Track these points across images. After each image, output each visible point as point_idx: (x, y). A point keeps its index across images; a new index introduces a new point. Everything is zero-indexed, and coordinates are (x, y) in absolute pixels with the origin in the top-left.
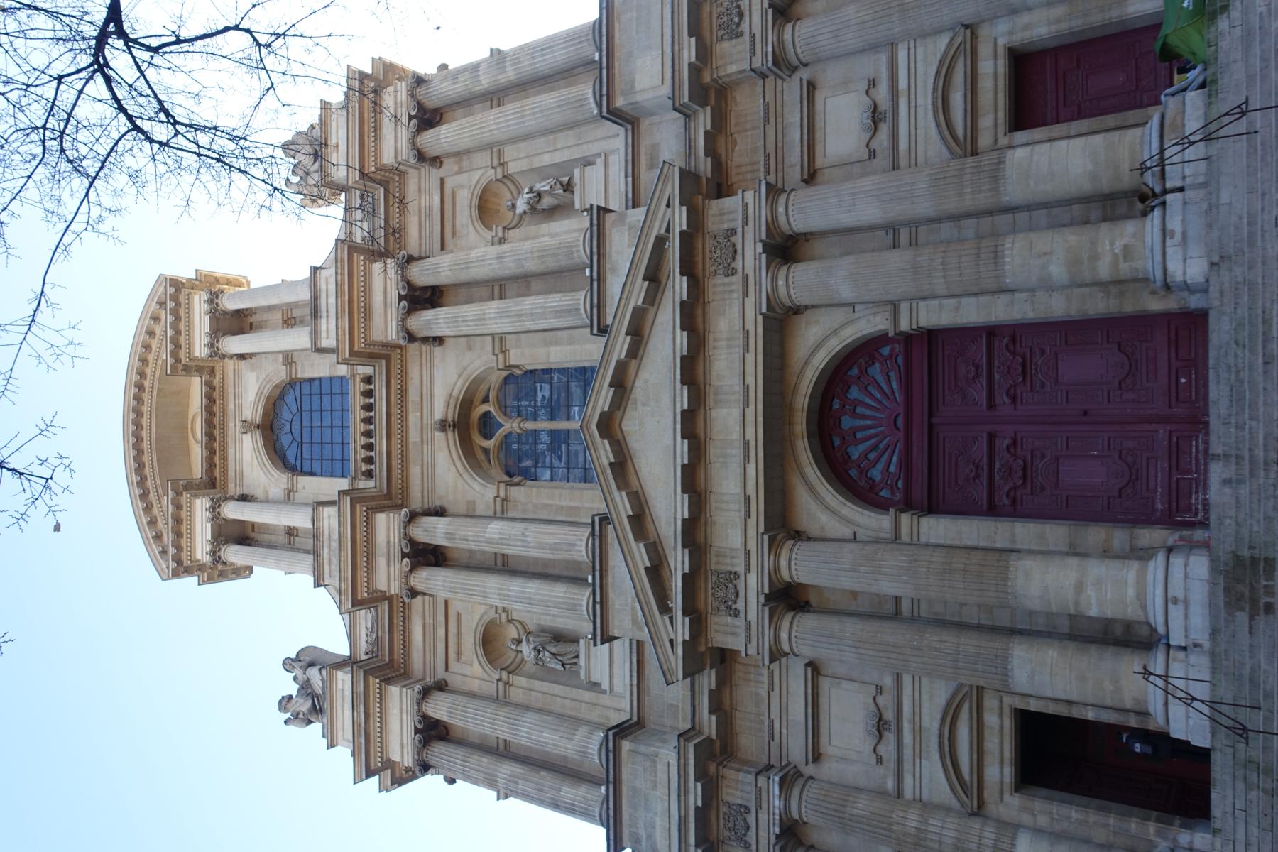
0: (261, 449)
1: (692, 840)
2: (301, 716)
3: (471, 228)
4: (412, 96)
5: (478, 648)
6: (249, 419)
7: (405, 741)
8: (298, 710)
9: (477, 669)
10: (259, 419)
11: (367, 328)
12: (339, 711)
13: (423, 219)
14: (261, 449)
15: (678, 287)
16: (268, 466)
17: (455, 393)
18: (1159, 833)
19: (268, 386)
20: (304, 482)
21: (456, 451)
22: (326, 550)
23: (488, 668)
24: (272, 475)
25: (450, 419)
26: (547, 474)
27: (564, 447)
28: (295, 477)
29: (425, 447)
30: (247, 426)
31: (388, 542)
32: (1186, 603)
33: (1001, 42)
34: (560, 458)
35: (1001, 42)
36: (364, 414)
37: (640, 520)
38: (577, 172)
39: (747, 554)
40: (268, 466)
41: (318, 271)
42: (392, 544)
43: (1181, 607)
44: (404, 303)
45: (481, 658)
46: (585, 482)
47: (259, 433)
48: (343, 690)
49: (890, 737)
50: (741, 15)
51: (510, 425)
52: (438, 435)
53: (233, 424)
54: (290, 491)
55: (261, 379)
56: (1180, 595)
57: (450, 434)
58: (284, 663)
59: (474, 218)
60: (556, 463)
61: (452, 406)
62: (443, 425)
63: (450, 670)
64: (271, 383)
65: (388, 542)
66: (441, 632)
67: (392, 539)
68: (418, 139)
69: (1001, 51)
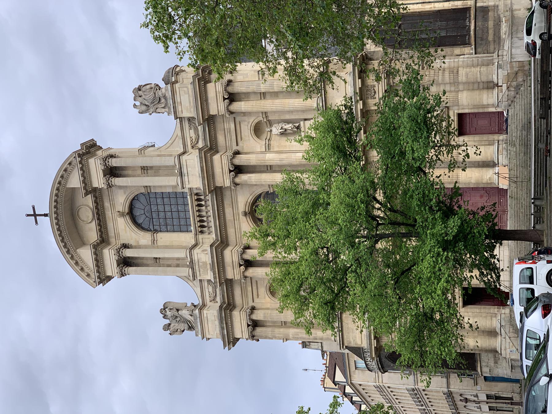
0: (130, 223)
1: (373, 338)
2: (179, 330)
3: (251, 138)
4: (225, 90)
5: (268, 292)
6: (121, 210)
7: (243, 330)
8: (177, 328)
9: (268, 299)
10: (127, 210)
11: (214, 182)
12: (206, 325)
14: (130, 223)
16: (136, 230)
17: (249, 201)
18: (498, 311)
19: (132, 196)
20: (160, 235)
22: (197, 266)
23: (273, 298)
24: (140, 234)
25: (247, 211)
28: (155, 234)
29: (236, 222)
30: (122, 214)
31: (233, 261)
32: (504, 260)
33: (456, 112)
35: (456, 112)
36: (197, 208)
38: (302, 123)
40: (136, 230)
41: (181, 157)
42: (234, 262)
43: (503, 261)
44: (232, 173)
45: (269, 296)
47: (128, 217)
50: (375, 92)
52: (243, 218)
53: (111, 212)
54: (154, 241)
55: (127, 195)
56: (502, 259)
57: (248, 217)
58: (163, 311)
59: (253, 135)
61: (247, 206)
62: (245, 214)
63: (254, 302)
64: (133, 194)
65: (233, 261)
67: (234, 260)
69: (455, 114)
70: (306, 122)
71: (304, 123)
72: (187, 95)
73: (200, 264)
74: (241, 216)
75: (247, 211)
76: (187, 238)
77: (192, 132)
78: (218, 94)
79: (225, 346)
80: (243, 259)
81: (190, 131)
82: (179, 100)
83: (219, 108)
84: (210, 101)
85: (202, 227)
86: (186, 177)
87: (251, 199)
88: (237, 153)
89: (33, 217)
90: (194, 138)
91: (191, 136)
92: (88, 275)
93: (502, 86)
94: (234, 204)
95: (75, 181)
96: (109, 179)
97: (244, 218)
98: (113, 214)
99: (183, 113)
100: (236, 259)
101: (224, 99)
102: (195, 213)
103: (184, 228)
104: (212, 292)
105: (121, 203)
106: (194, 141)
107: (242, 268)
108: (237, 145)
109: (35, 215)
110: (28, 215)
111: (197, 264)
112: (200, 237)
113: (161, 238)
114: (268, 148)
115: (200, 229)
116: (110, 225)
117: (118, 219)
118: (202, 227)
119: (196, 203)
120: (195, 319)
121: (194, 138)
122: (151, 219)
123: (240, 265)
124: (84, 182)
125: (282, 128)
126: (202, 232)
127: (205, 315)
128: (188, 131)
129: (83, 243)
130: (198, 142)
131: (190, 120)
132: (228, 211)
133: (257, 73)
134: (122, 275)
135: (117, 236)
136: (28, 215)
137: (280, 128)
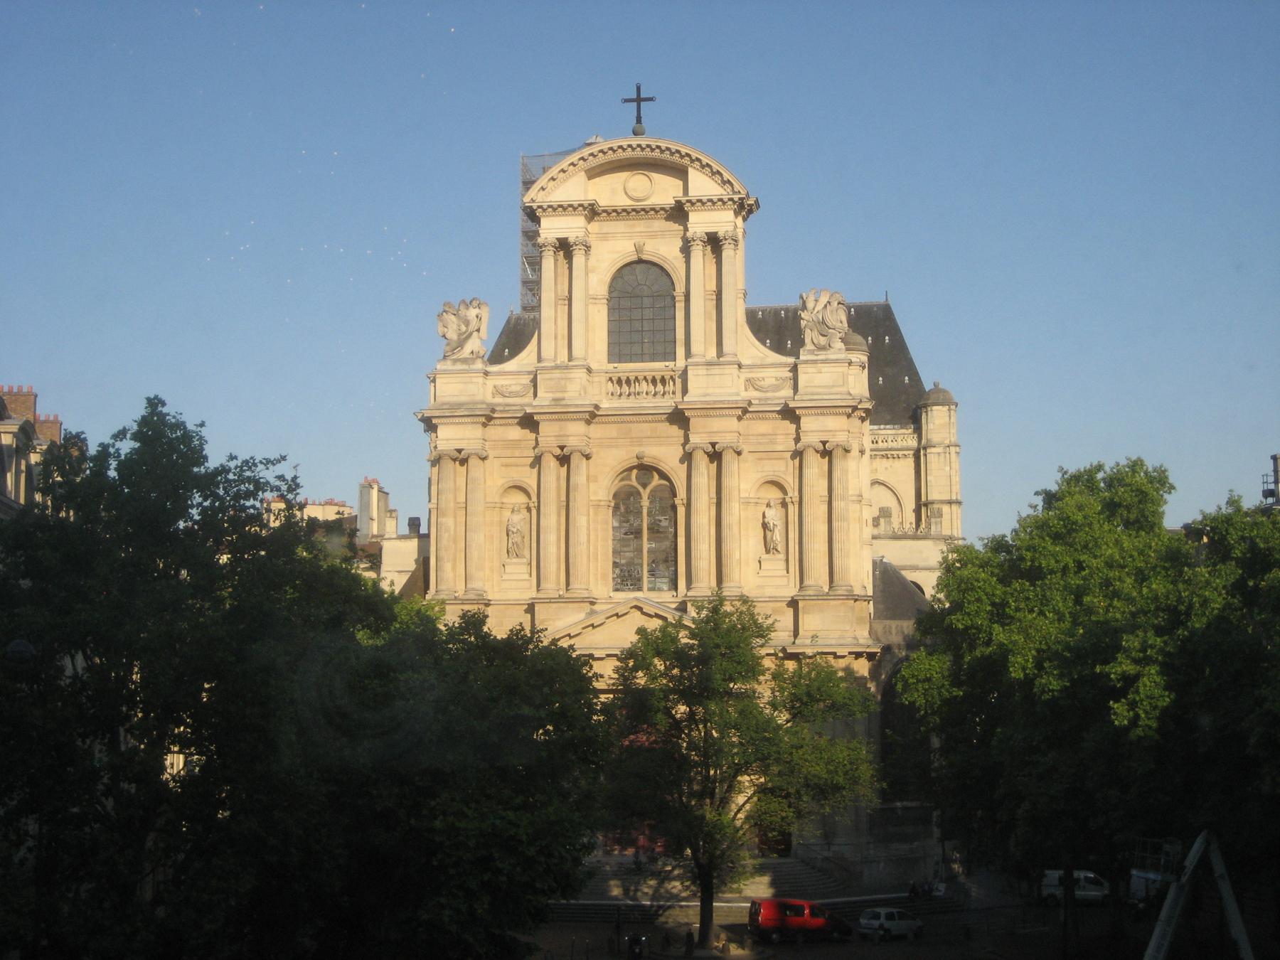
8: (449, 327)
9: (500, 482)
10: (645, 257)
13: (769, 437)
17: (662, 464)
21: (627, 465)
26: (616, 524)
27: (632, 536)
30: (638, 249)
34: (626, 534)
46: (613, 552)
47: (634, 258)
48: (472, 382)
51: (645, 494)
55: (673, 261)
60: (623, 531)
66: (517, 453)
68: (811, 449)
71: (781, 560)
72: (831, 384)
73: (563, 382)
74: (637, 450)
77: (773, 381)
78: (831, 433)
81: (774, 379)
82: (823, 370)
83: (811, 434)
84: (821, 418)
86: (705, 372)
87: (664, 467)
89: (635, 96)
90: (762, 383)
91: (766, 379)
93: (829, 850)
98: (639, 234)
99: (804, 375)
101: (824, 443)
102: (641, 374)
103: (618, 352)
104: (510, 390)
105: (658, 250)
106: (758, 383)
109: (639, 100)
110: (638, 89)
111: (563, 375)
112: (604, 378)
113: (599, 311)
114: (747, 502)
116: (619, 226)
117: (633, 242)
119: (658, 378)
120: (465, 361)
121: (762, 383)
122: (629, 295)
123: (562, 448)
127: (475, 380)
128: (774, 374)
130: (756, 390)
132: (645, 428)
133: (857, 493)
135: (604, 237)
136: (638, 89)
137: (775, 523)
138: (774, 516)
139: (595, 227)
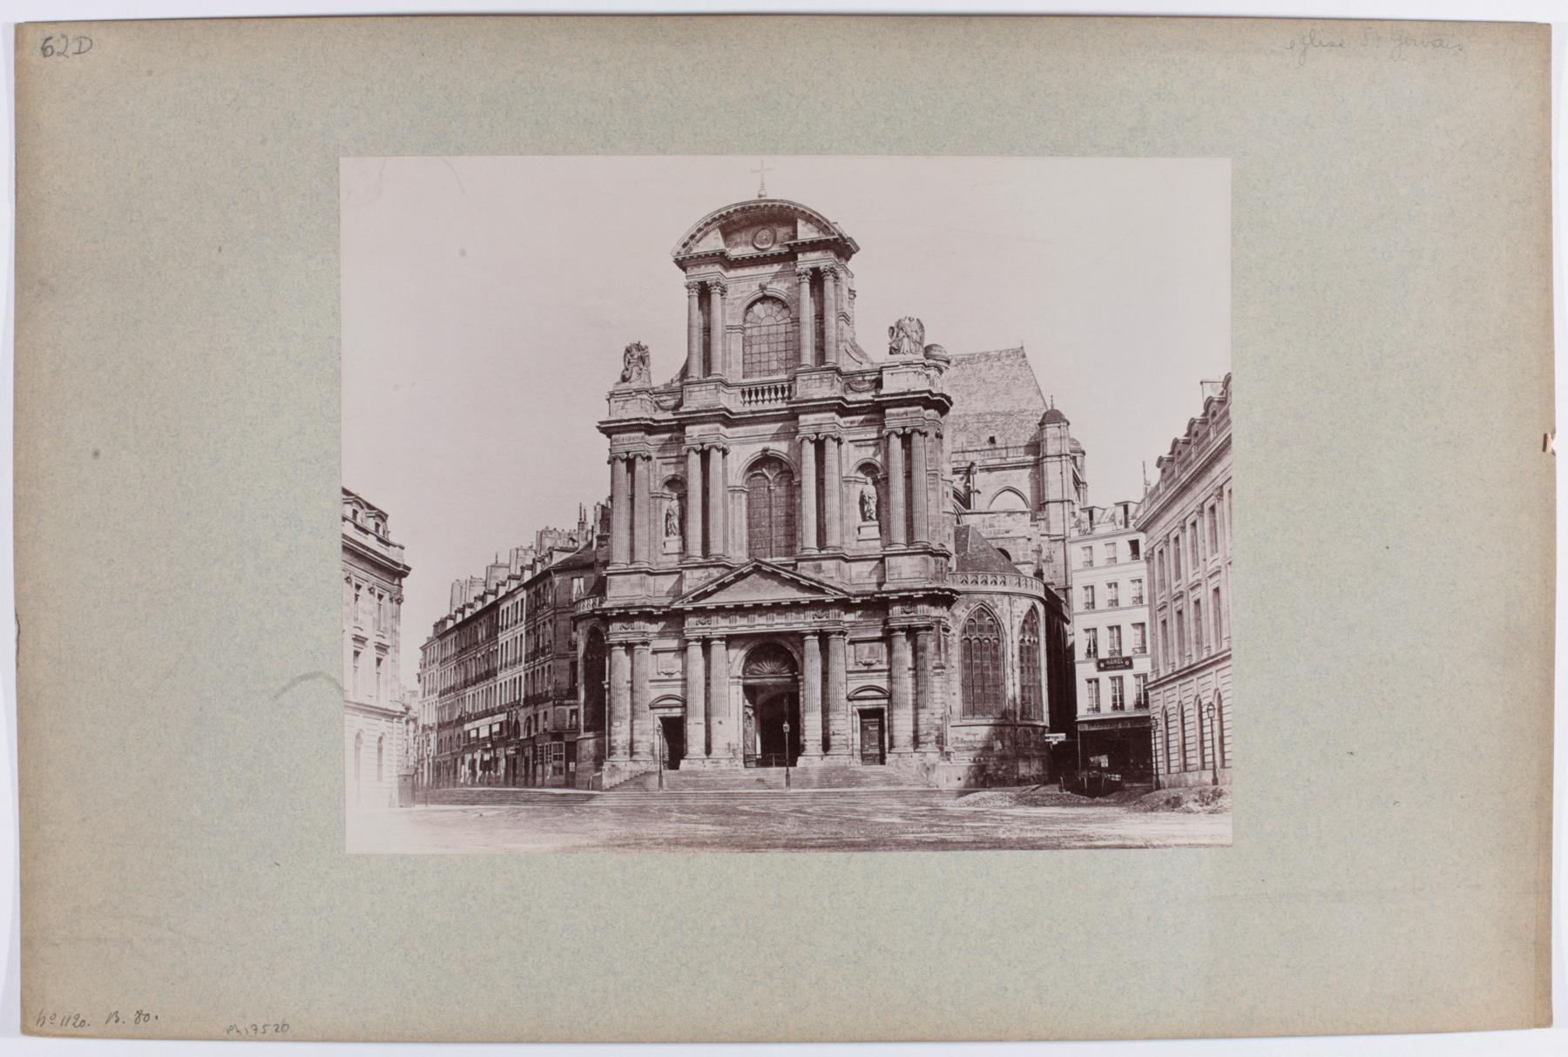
15: (805, 597)
37: (722, 586)
39: (717, 628)
49: (667, 677)
52: (759, 447)
70: (877, 528)
75: (770, 452)
76: (735, 374)
79: (601, 423)
80: (710, 449)
85: (749, 392)
88: (839, 441)
92: (685, 245)
94: (776, 437)
95: (806, 233)
96: (807, 275)
97: (761, 449)
100: (710, 440)
107: (700, 448)
108: (851, 441)
112: (737, 391)
115: (746, 389)
117: (759, 282)
118: (749, 392)
119: (779, 386)
124: (804, 244)
125: (870, 498)
126: (743, 393)
129: (726, 234)
131: (878, 383)
134: (688, 287)
135: (739, 279)
138: (870, 490)
139: (732, 273)
